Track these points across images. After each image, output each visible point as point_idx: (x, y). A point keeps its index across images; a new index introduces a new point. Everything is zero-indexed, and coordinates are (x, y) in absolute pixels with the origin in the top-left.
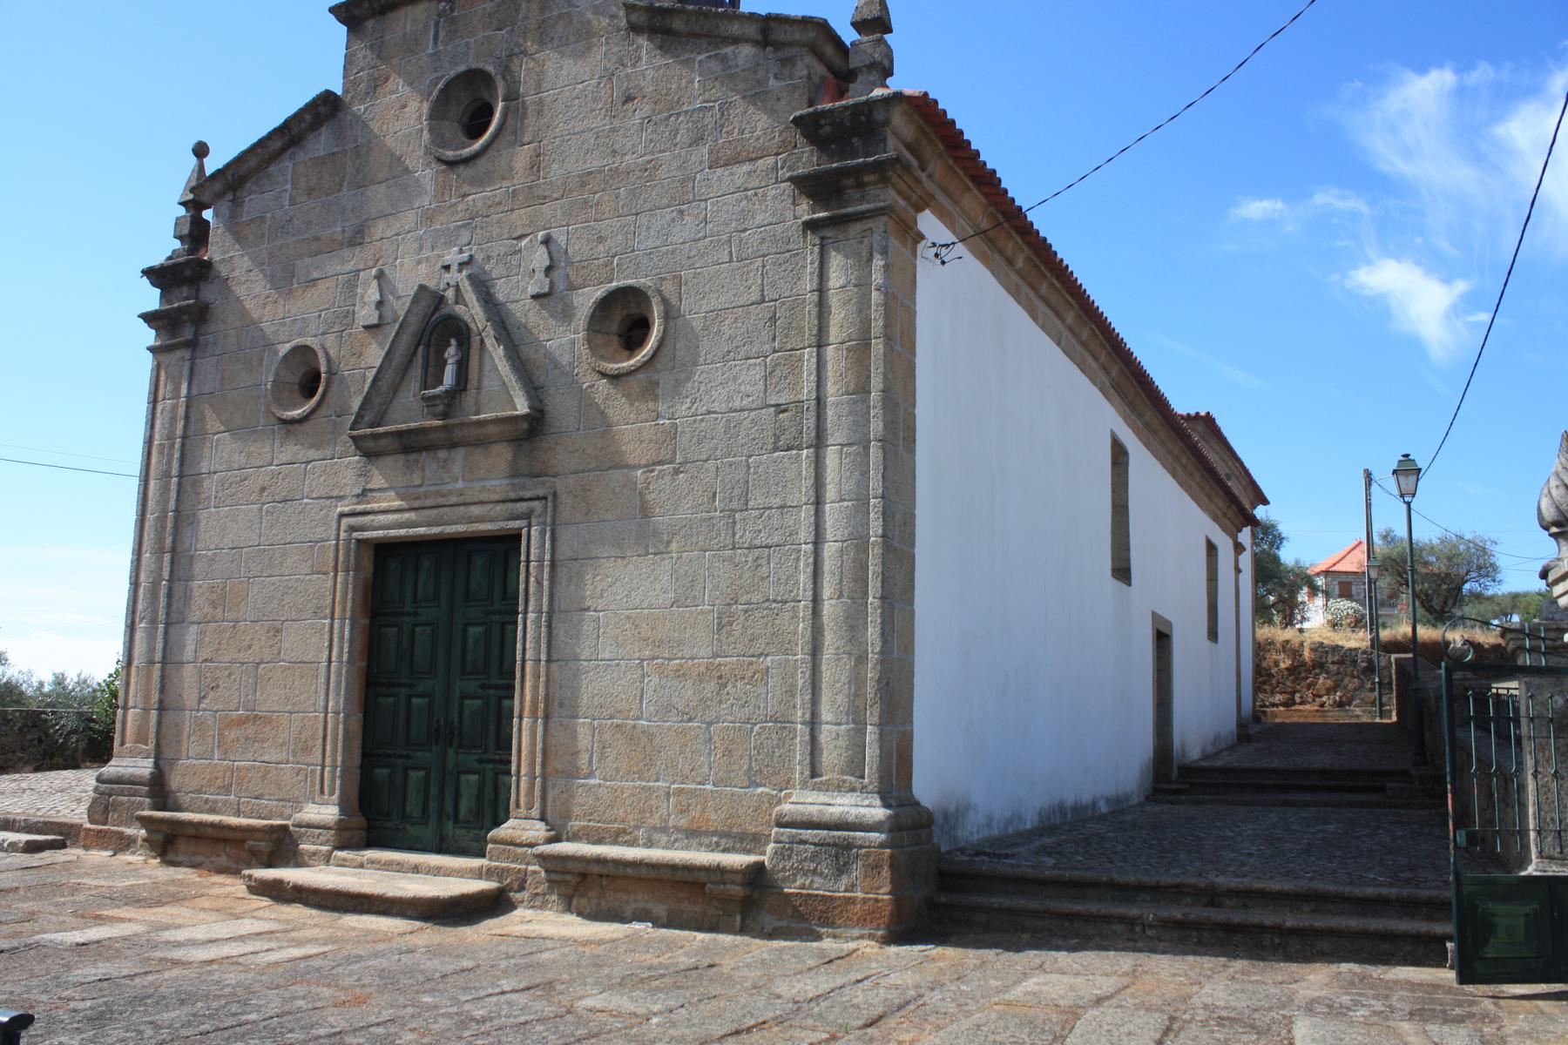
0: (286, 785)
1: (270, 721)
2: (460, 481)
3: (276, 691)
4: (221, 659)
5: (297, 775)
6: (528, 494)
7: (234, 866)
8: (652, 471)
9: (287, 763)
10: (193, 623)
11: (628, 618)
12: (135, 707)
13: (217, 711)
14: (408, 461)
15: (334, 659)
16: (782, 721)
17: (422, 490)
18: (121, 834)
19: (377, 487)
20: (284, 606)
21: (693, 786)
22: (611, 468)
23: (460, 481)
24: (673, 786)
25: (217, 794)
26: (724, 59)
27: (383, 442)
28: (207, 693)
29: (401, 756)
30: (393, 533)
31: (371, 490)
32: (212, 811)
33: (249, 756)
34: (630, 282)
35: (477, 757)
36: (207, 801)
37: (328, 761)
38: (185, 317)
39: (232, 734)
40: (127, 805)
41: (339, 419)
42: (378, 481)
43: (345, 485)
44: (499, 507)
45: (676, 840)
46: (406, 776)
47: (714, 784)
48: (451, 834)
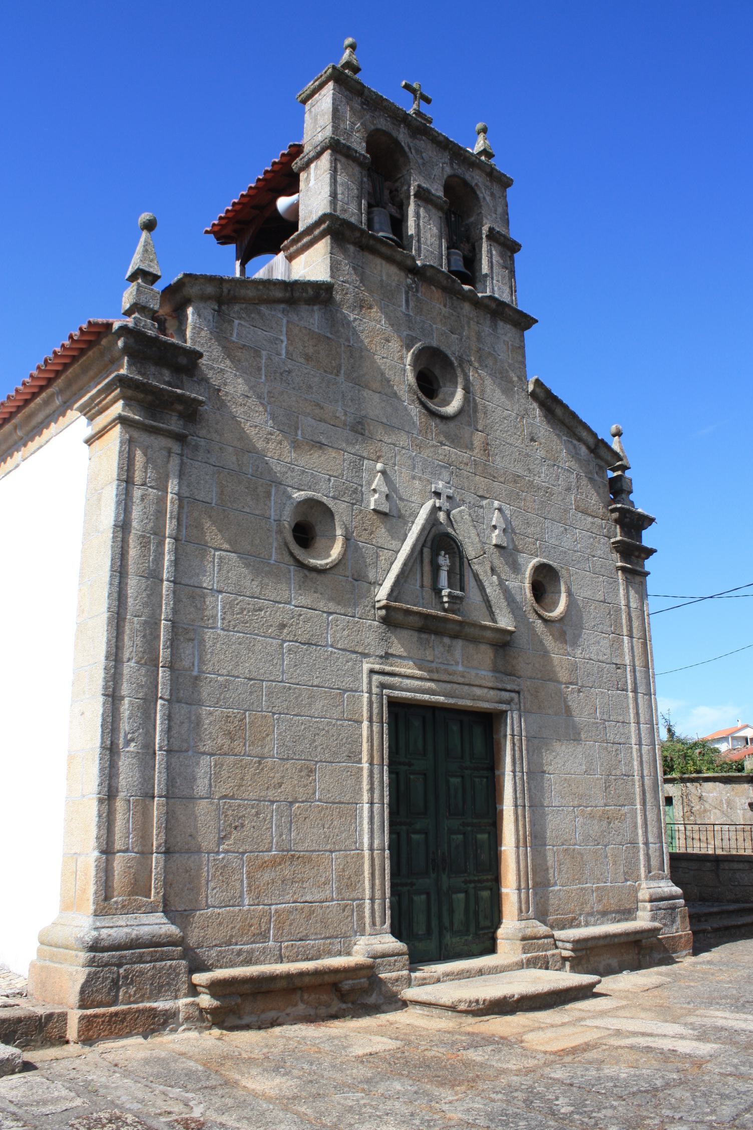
0: (332, 923)
1: (310, 860)
2: (460, 665)
3: (315, 830)
4: (245, 796)
5: (344, 911)
6: (509, 687)
7: (312, 1012)
8: (568, 688)
9: (332, 900)
10: (204, 753)
11: (566, 779)
12: (126, 851)
13: (243, 853)
14: (421, 638)
15: (376, 801)
16: (634, 843)
17: (434, 665)
18: (154, 1009)
19: (398, 653)
20: (316, 747)
21: (603, 885)
22: (549, 680)
23: (460, 665)
24: (594, 886)
25: (252, 943)
26: (575, 447)
27: (411, 619)
28: (230, 833)
29: (406, 885)
30: (419, 696)
31: (393, 655)
32: (248, 962)
33: (288, 898)
34: (551, 563)
35: (463, 879)
36: (239, 953)
37: (378, 894)
38: (180, 407)
39: (267, 876)
40: (150, 973)
41: (356, 583)
42: (397, 649)
43: (369, 645)
44: (492, 692)
45: (598, 920)
46: (411, 901)
47: (611, 883)
48: (449, 944)
